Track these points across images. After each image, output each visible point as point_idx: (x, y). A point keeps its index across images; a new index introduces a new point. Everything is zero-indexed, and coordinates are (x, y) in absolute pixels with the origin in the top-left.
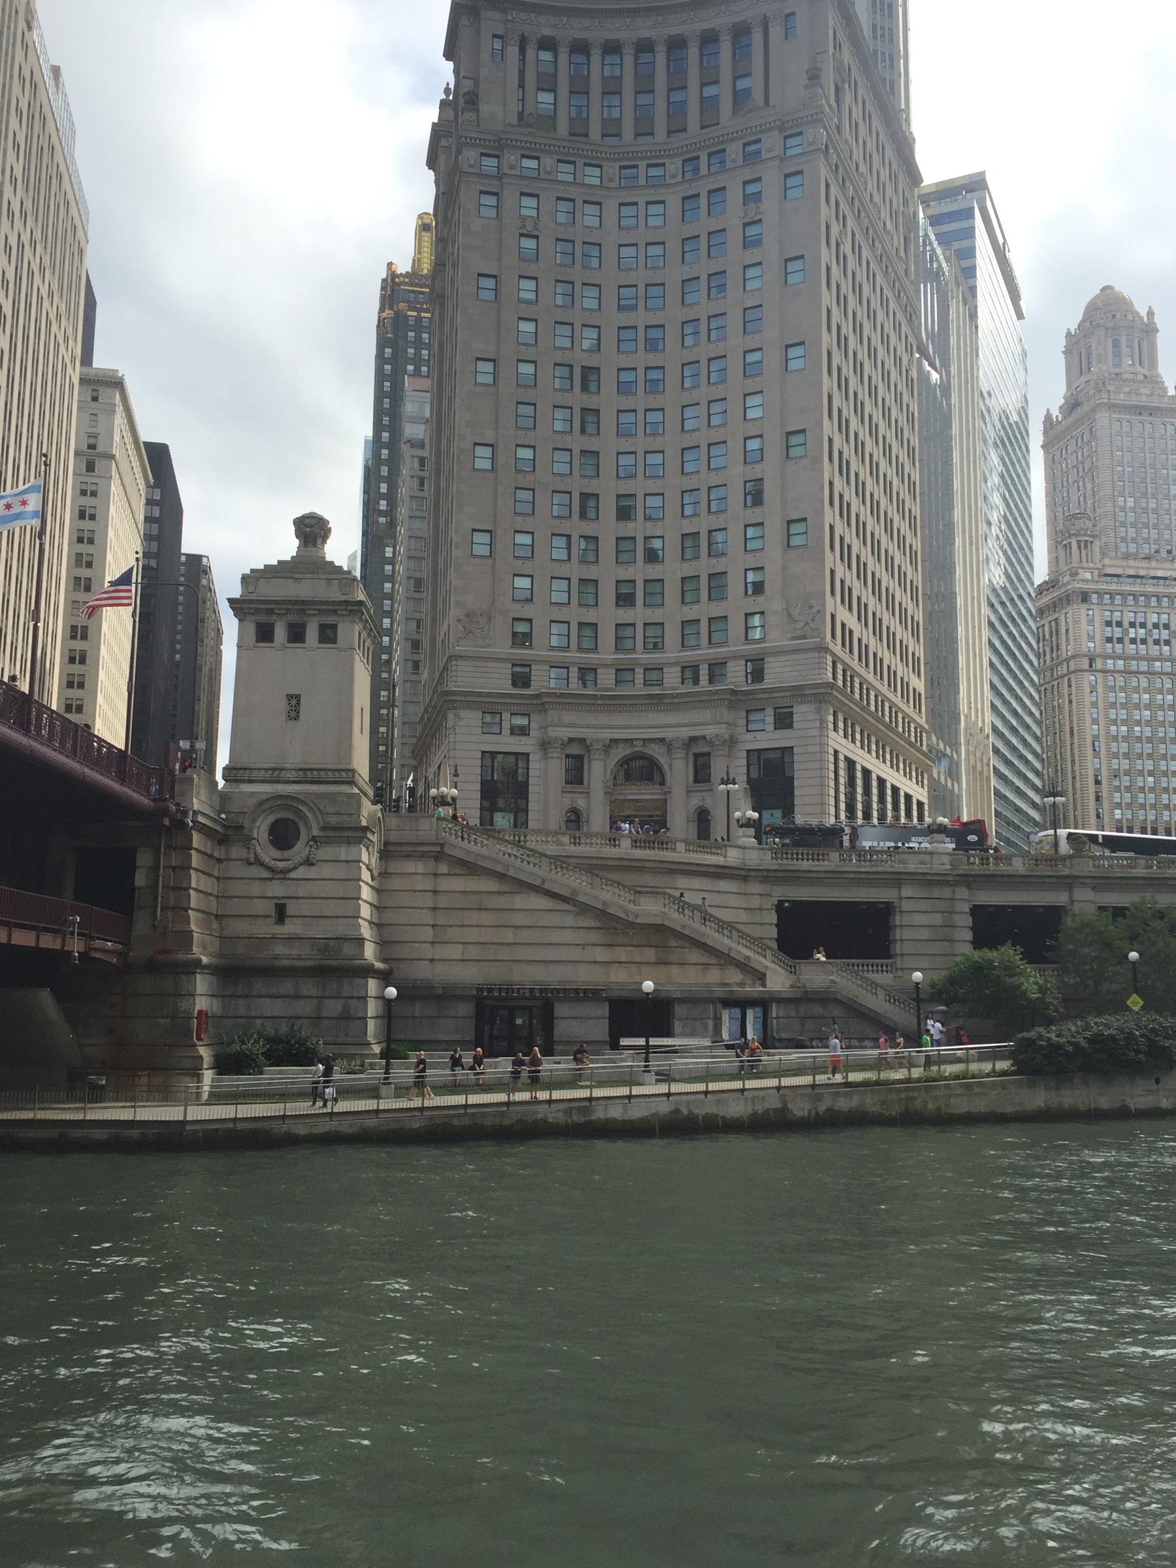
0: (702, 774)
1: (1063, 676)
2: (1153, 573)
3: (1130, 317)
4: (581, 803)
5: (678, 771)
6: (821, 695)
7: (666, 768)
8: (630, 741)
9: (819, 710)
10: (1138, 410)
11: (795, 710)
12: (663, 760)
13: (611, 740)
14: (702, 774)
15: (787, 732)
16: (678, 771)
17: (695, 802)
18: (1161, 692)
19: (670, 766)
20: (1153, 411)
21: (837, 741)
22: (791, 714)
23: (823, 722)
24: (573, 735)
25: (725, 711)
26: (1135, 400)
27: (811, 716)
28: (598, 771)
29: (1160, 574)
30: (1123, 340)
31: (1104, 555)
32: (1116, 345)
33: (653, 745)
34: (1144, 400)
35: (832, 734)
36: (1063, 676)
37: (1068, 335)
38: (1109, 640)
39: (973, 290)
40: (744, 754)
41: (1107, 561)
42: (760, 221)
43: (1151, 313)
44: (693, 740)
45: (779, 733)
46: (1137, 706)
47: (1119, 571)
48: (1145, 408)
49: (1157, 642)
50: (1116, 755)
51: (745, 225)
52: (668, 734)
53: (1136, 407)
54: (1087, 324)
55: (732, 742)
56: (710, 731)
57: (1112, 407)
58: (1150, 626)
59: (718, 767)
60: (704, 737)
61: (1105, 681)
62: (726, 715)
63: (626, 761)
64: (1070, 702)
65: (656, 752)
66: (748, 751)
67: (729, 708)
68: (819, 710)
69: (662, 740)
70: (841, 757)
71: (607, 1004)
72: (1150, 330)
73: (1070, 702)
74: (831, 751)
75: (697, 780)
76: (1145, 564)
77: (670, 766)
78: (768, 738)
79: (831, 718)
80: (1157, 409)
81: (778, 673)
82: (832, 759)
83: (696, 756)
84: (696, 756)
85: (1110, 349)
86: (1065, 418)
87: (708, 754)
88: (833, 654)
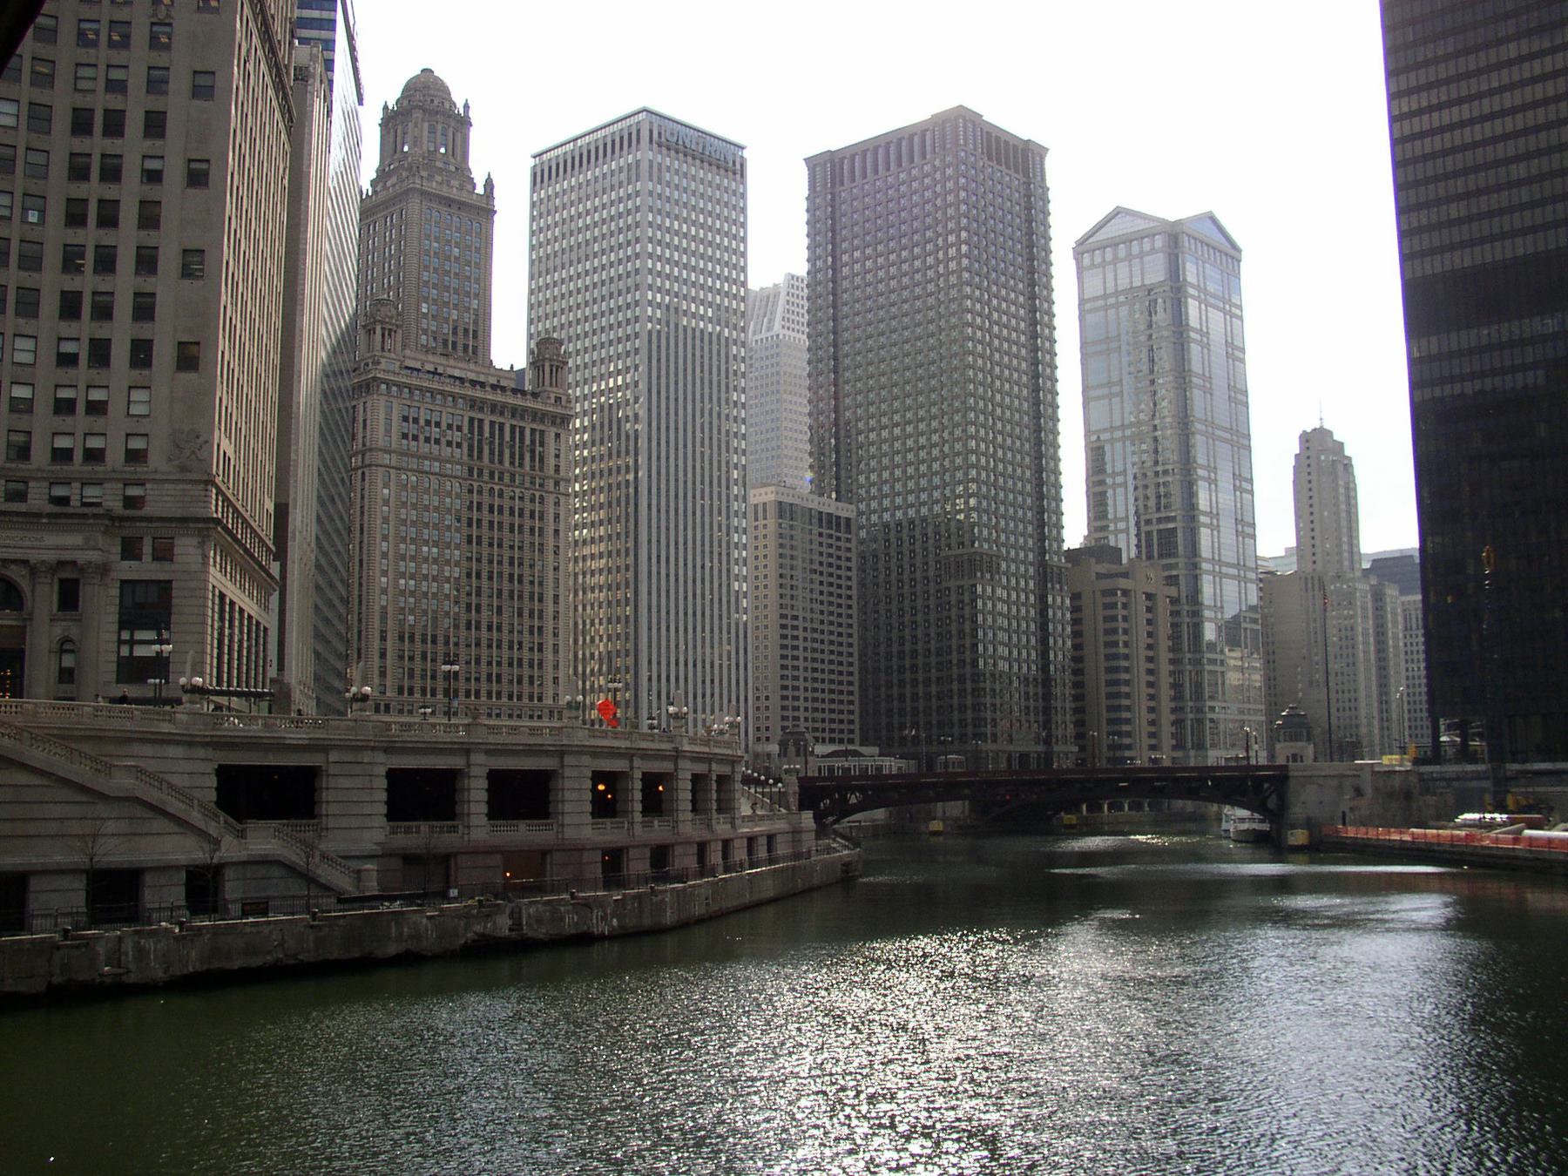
1: (356, 469)
2: (450, 371)
3: (447, 105)
6: (204, 527)
9: (202, 544)
10: (449, 202)
11: (176, 542)
12: (24, 584)
15: (166, 565)
16: (43, 599)
17: (58, 631)
18: (449, 495)
19: (33, 591)
20: (461, 205)
21: (217, 578)
22: (172, 546)
23: (205, 557)
25: (100, 537)
26: (445, 191)
27: (192, 550)
29: (457, 373)
30: (439, 127)
31: (404, 346)
32: (432, 131)
33: (13, 567)
34: (454, 193)
36: (356, 469)
37: (386, 107)
38: (405, 436)
39: (331, 82)
41: (408, 352)
42: (170, 25)
43: (466, 107)
44: (61, 564)
45: (156, 566)
46: (427, 508)
47: (418, 366)
48: (454, 201)
49: (449, 444)
50: (403, 558)
51: (153, 24)
52: (34, 556)
53: (446, 198)
54: (405, 103)
55: (104, 569)
56: (82, 557)
57: (423, 193)
58: (444, 426)
59: (87, 593)
60: (74, 563)
61: (398, 476)
62: (101, 540)
64: (363, 497)
65: (17, 574)
66: (123, 582)
67: (105, 533)
68: (202, 544)
69: (25, 562)
71: (84, 877)
72: (464, 123)
73: (363, 497)
76: (443, 360)
77: (33, 591)
78: (145, 569)
80: (464, 204)
81: (160, 501)
83: (62, 581)
84: (62, 581)
85: (426, 133)
86: (374, 192)
87: (76, 582)
88: (218, 488)
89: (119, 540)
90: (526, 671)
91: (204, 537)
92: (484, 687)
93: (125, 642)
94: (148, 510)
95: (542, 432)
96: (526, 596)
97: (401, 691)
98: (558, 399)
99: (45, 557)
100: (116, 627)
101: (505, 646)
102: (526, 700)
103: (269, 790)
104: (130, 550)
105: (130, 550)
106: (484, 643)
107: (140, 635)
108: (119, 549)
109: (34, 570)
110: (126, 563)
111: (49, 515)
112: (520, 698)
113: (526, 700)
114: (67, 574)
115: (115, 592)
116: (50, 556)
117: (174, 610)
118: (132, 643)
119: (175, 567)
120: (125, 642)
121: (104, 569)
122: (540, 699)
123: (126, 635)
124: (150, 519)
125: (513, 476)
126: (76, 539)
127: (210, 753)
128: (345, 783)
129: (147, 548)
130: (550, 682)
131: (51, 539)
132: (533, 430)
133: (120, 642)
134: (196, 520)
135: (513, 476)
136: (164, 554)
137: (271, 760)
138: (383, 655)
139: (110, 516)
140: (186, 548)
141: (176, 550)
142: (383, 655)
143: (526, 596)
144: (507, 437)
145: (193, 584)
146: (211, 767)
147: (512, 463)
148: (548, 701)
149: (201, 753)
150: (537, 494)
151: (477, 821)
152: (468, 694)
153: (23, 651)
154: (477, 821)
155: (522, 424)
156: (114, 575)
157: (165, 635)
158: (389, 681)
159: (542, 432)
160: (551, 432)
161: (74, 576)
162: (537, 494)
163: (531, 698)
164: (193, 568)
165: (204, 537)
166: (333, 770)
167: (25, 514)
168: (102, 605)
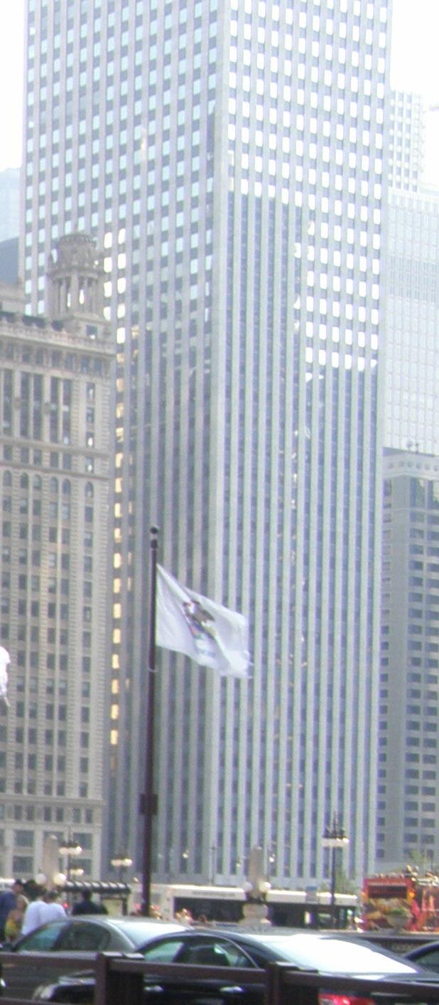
95: (68, 383)
96: (43, 634)
98: (91, 330)
102: (40, 793)
112: (31, 790)
113: (40, 793)
122: (61, 791)
125: (25, 451)
132: (55, 381)
135: (25, 451)
143: (43, 634)
144: (17, 391)
147: (24, 432)
148: (73, 794)
150: (61, 479)
155: (39, 371)
159: (68, 383)
160: (82, 381)
162: (61, 479)
163: (48, 790)
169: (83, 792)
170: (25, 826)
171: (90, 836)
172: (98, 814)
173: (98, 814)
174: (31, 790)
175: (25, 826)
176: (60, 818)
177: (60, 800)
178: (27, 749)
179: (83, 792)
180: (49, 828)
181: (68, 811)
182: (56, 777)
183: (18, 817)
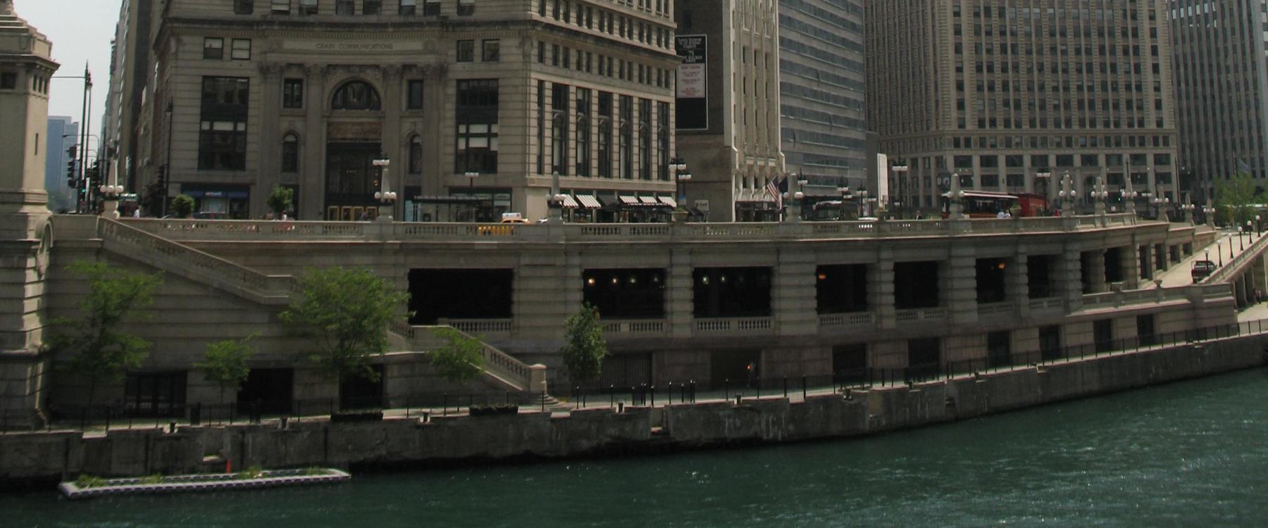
0: (415, 102)
4: (299, 125)
5: (393, 95)
7: (382, 95)
8: (347, 67)
9: (522, 44)
12: (378, 85)
13: (329, 66)
14: (415, 102)
15: (493, 66)
16: (393, 95)
17: (407, 127)
23: (526, 56)
24: (292, 61)
27: (515, 51)
28: (316, 95)
33: (369, 71)
35: (535, 64)
40: (454, 83)
44: (407, 67)
45: (484, 66)
52: (385, 60)
55: (442, 71)
60: (415, 66)
63: (344, 86)
66: (459, 81)
69: (377, 67)
70: (548, 85)
74: (534, 83)
75: (410, 106)
78: (476, 69)
79: (535, 52)
82: (534, 90)
84: (411, 82)
87: (421, 81)
89: (454, 44)
90: (1123, 95)
91: (525, 39)
92: (1075, 115)
93: (462, 135)
94: (477, 15)
97: (981, 123)
99: (392, 62)
100: (452, 122)
101: (1096, 69)
102: (1124, 127)
103: (464, 293)
104: (465, 54)
105: (465, 54)
106: (1072, 67)
107: (476, 129)
108: (453, 52)
109: (385, 72)
110: (460, 65)
111: (395, 25)
112: (1117, 125)
113: (1124, 127)
114: (414, 75)
115: (452, 90)
116: (396, 60)
117: (501, 105)
118: (468, 136)
119: (501, 66)
120: (462, 135)
121: (442, 71)
122: (1141, 124)
123: (462, 129)
124: (476, 24)
126: (417, 45)
127: (401, 259)
128: (538, 285)
129: (477, 51)
130: (1152, 106)
131: (398, 46)
133: (458, 135)
134: (515, 22)
136: (493, 55)
137: (463, 264)
138: (960, 87)
139: (445, 24)
140: (510, 48)
141: (502, 51)
142: (960, 87)
145: (517, 82)
146: (403, 272)
148: (1151, 125)
149: (390, 259)
151: (680, 319)
152: (1057, 125)
153: (379, 145)
154: (680, 319)
156: (451, 75)
157: (495, 129)
158: (968, 114)
161: (420, 77)
163: (1131, 125)
164: (516, 66)
165: (525, 39)
166: (524, 272)
167: (375, 25)
168: (445, 102)
169: (1159, 123)
170: (1114, 151)
171: (1145, 155)
172: (1173, 140)
173: (1172, 139)
174: (1043, 124)
175: (1114, 151)
176: (1142, 144)
177: (1141, 130)
178: (1110, 96)
179: (1159, 123)
180: (1110, 152)
181: (1149, 139)
182: (1136, 115)
183: (1108, 144)
